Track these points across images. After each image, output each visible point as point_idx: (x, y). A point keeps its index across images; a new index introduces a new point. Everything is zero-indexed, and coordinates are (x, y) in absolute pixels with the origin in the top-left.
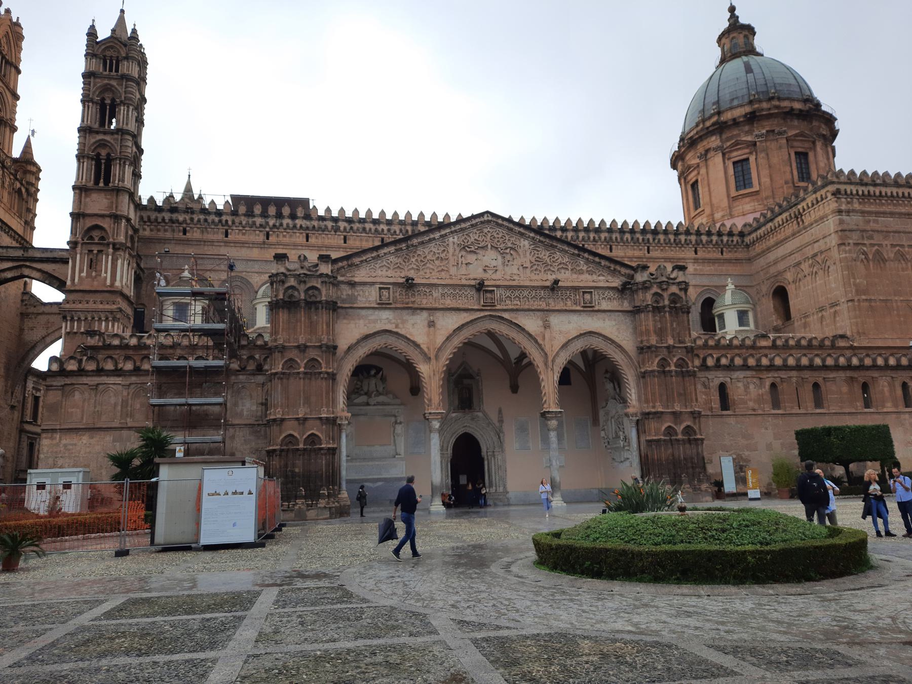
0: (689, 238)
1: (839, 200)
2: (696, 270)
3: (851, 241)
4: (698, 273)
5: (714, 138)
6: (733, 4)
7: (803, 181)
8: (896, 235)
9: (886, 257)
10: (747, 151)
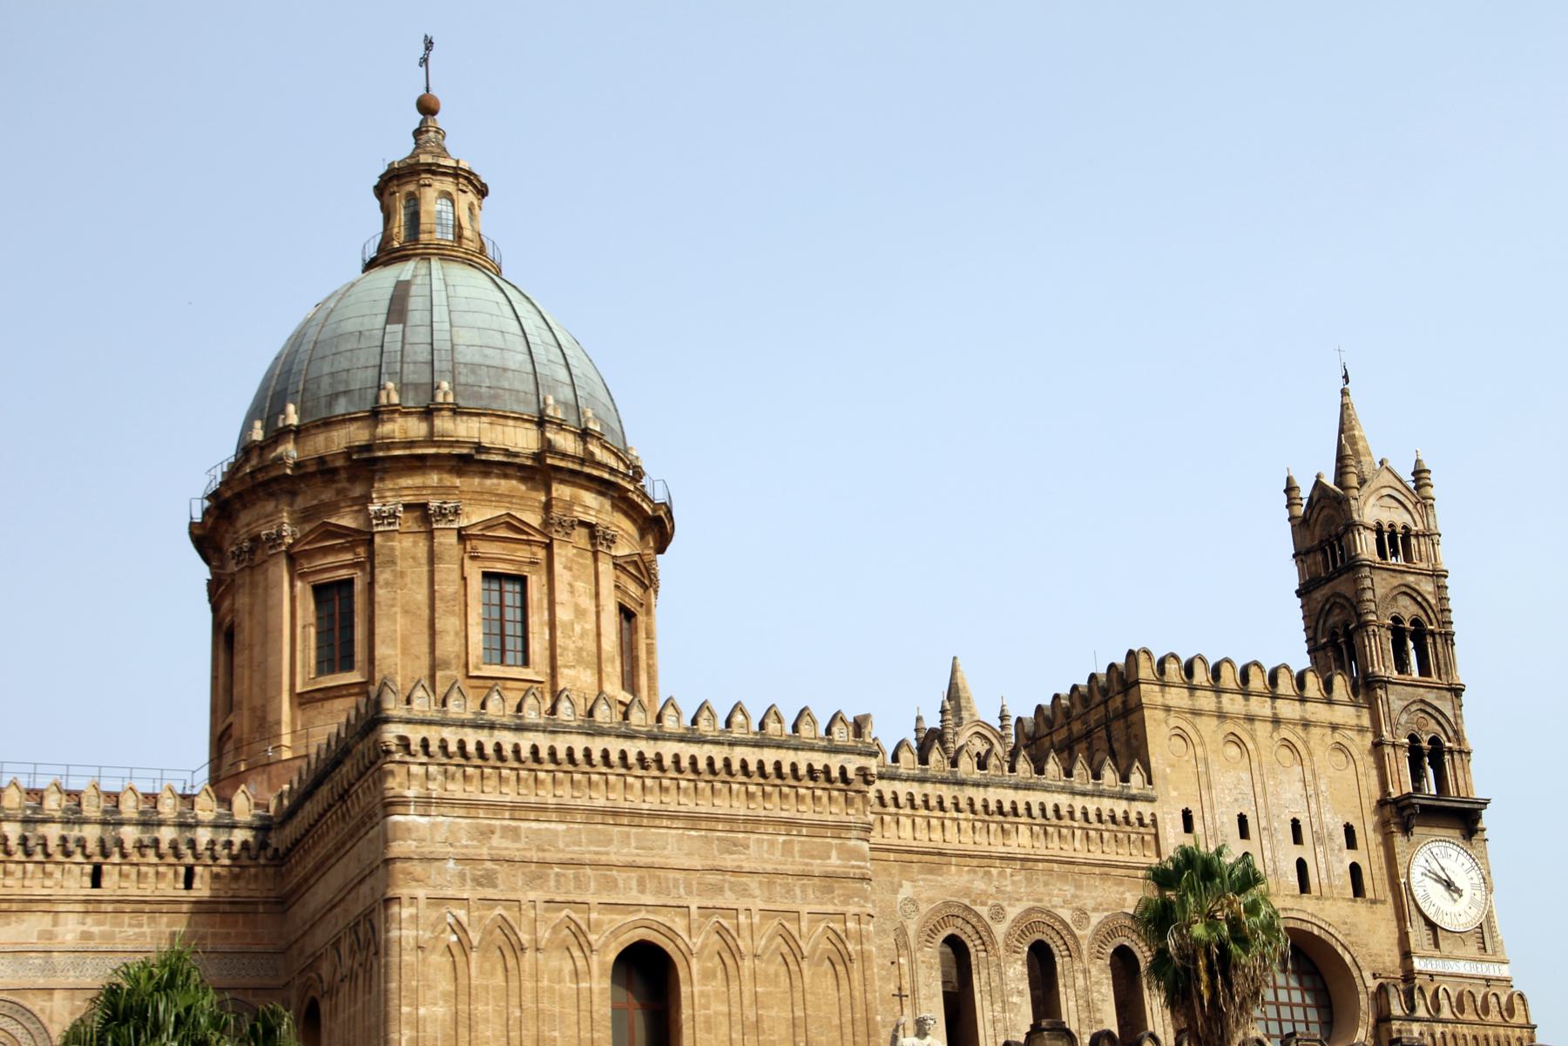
0: (75, 832)
1: (403, 769)
2: (87, 936)
3: (421, 893)
4: (91, 945)
6: (434, 91)
7: (502, 662)
8: (570, 872)
9: (525, 938)
10: (347, 557)
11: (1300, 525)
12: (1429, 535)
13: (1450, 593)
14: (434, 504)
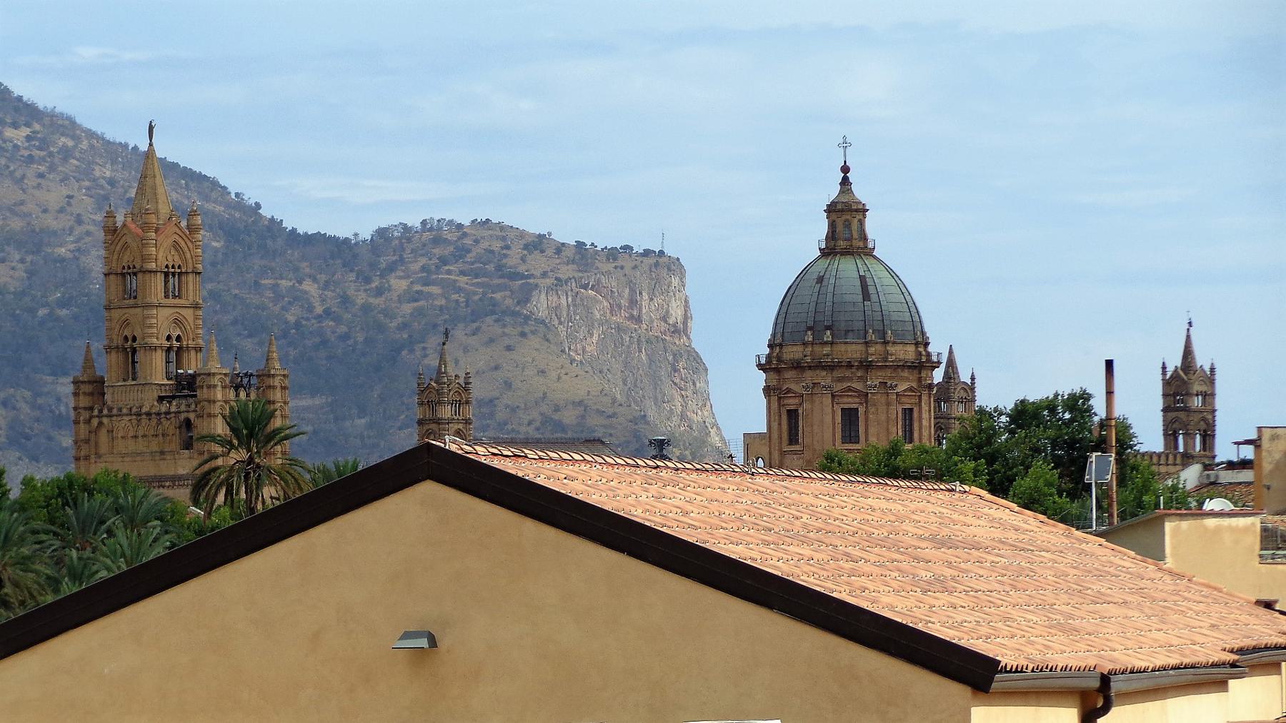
5: (824, 373)
10: (857, 400)
11: (1167, 383)
12: (1213, 395)
13: (1217, 418)
14: (889, 383)
